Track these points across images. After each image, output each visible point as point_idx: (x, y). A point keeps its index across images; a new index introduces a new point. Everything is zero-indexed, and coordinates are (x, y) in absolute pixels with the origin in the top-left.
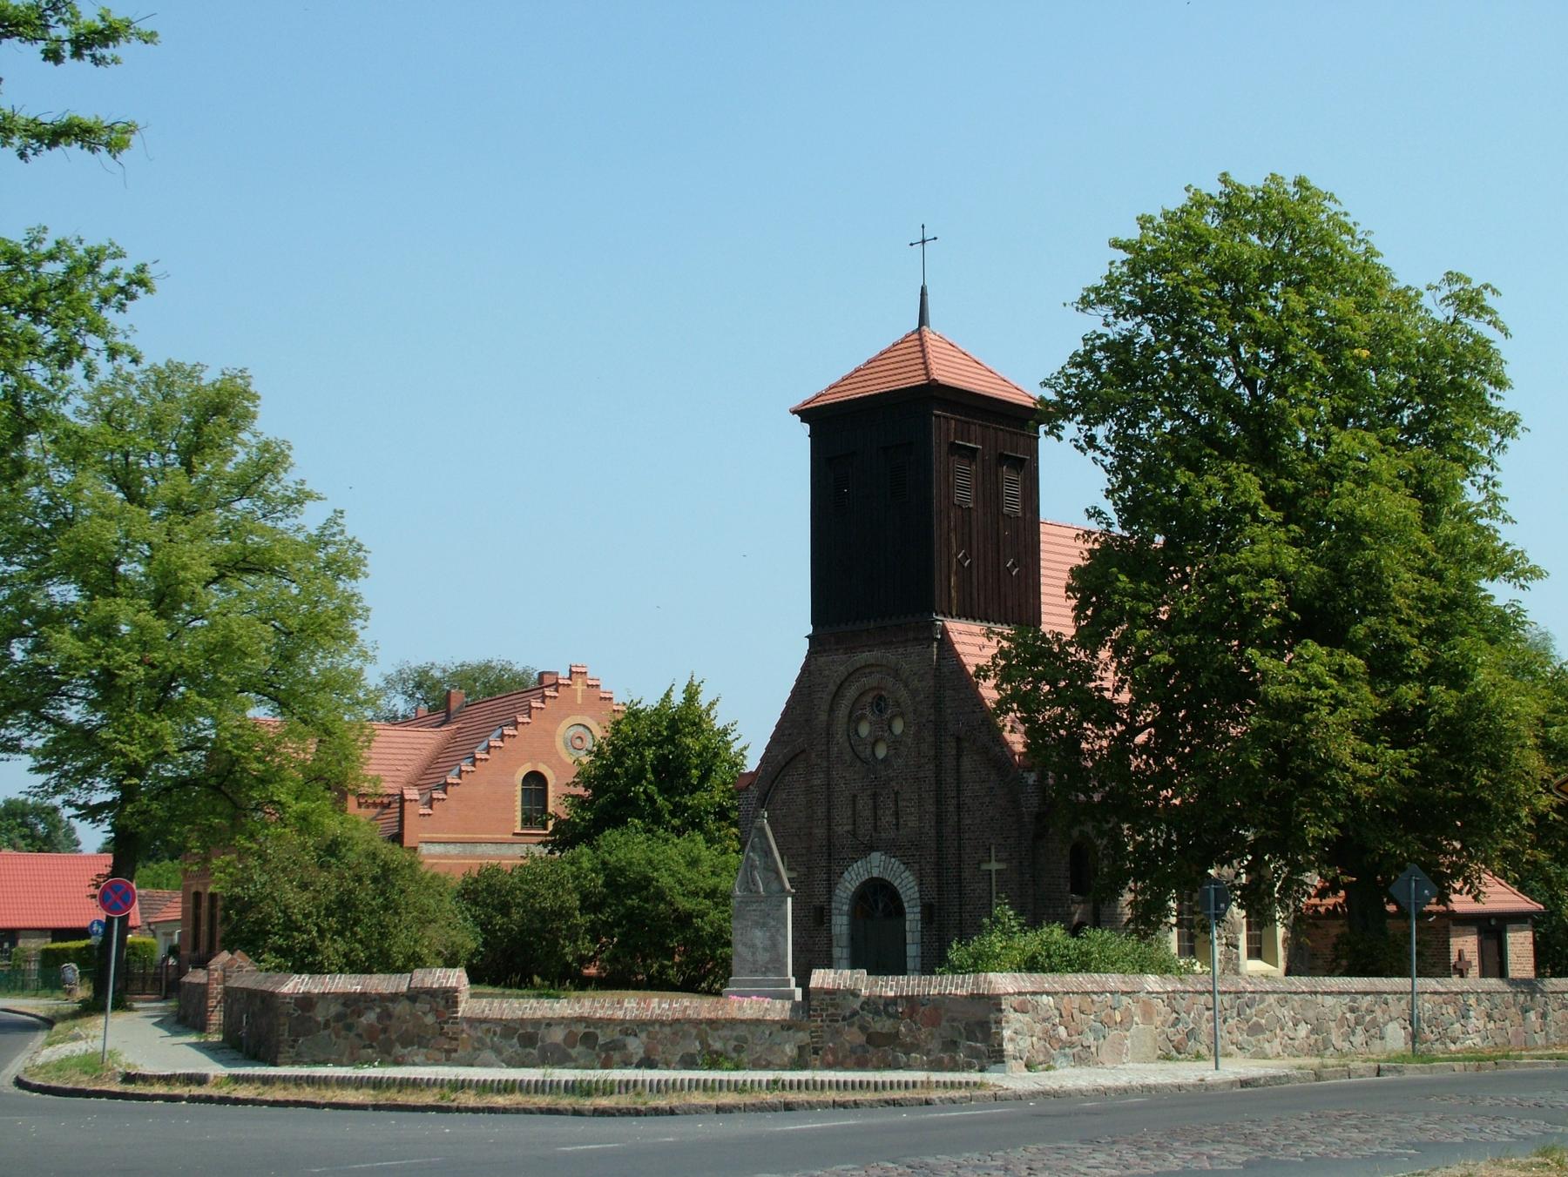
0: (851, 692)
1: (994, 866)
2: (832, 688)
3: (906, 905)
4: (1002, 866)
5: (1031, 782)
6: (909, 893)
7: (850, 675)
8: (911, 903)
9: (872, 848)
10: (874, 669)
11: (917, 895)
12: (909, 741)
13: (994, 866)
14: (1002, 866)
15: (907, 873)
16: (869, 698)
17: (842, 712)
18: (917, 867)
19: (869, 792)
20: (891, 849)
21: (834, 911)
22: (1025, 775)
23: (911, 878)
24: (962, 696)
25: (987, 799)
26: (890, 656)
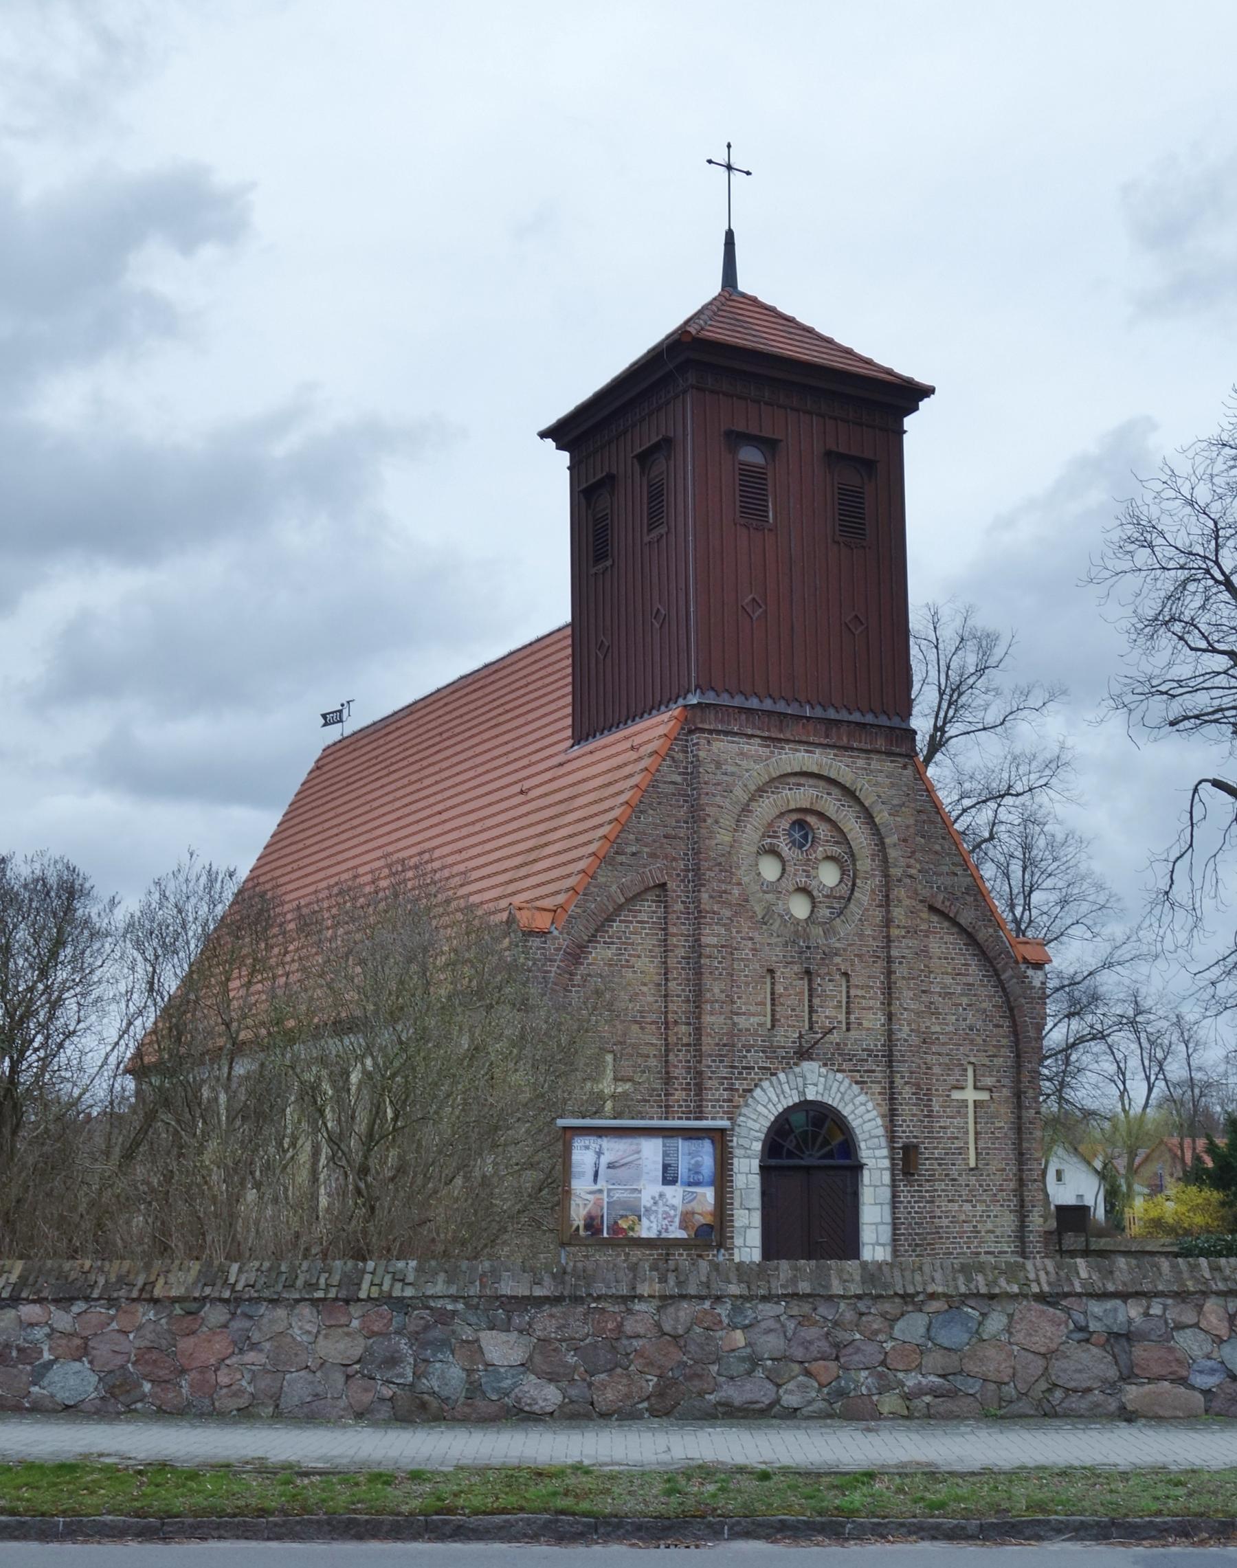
0: (766, 808)
1: (970, 1095)
2: (740, 794)
3: (863, 1145)
4: (984, 1096)
5: (1037, 983)
6: (867, 1127)
7: (772, 780)
8: (870, 1143)
9: (804, 1054)
10: (802, 780)
11: (881, 1131)
12: (865, 900)
13: (970, 1095)
14: (984, 1096)
15: (862, 1098)
16: (785, 824)
17: (751, 835)
18: (877, 1088)
19: (796, 968)
20: (838, 1060)
21: (737, 1152)
22: (1030, 972)
23: (870, 1105)
24: (938, 847)
25: (965, 1001)
26: (841, 767)
